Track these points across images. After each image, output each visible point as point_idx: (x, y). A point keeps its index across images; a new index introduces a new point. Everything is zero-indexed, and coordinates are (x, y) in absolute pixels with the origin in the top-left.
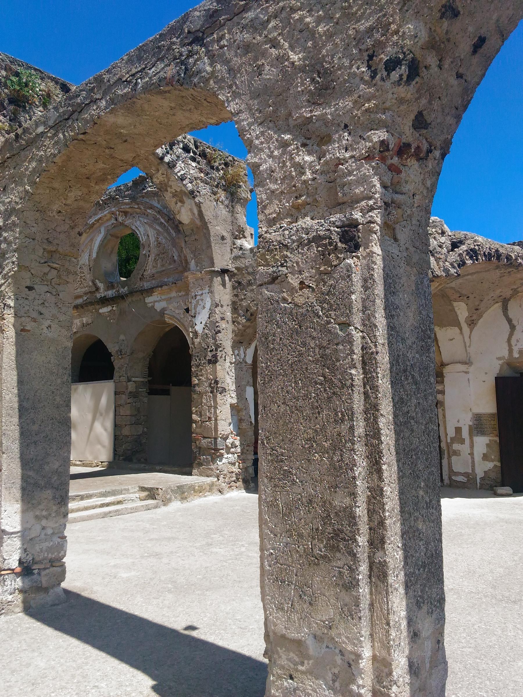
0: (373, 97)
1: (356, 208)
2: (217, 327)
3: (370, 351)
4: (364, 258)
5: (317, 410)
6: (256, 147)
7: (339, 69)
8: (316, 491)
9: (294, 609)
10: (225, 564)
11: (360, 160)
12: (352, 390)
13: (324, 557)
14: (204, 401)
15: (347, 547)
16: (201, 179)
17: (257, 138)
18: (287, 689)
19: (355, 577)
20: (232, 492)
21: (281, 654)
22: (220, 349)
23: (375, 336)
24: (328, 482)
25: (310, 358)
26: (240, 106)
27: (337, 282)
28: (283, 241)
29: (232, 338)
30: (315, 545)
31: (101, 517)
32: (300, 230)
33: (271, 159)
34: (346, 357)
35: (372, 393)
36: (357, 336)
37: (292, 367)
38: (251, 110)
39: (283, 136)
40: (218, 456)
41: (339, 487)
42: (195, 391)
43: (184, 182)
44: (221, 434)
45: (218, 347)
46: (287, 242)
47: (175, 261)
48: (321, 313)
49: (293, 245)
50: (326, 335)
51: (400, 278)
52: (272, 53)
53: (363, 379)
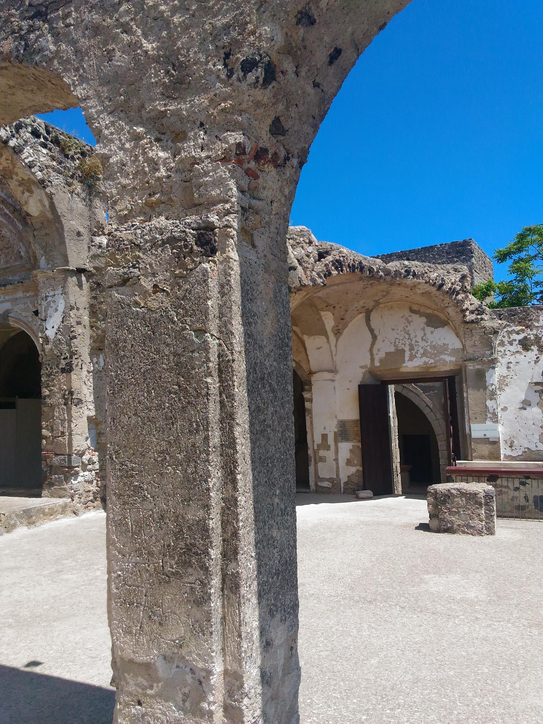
0: (229, 97)
1: (213, 210)
2: (72, 332)
3: (227, 359)
4: (221, 263)
5: (171, 420)
6: (106, 137)
7: (195, 64)
8: (168, 506)
9: (143, 632)
10: (76, 590)
11: (216, 161)
12: (208, 399)
13: (177, 573)
14: (56, 414)
15: (199, 561)
16: (53, 168)
17: (107, 128)
18: (135, 716)
19: (207, 592)
21: (129, 680)
22: (76, 356)
23: (232, 343)
24: (181, 496)
25: (164, 366)
26: (88, 92)
27: (193, 287)
28: (134, 241)
29: (90, 345)
30: (167, 562)
32: (153, 229)
33: (122, 152)
34: (202, 365)
35: (228, 402)
36: (213, 343)
37: (144, 376)
38: (100, 97)
39: (135, 128)
40: (72, 475)
41: (192, 500)
42: (45, 403)
43: (33, 170)
44: (76, 450)
45: (72, 354)
46: (139, 242)
47: (21, 257)
48: (176, 319)
49: (146, 245)
50: (181, 342)
51: (258, 285)
52: (124, 39)
53: (219, 387)
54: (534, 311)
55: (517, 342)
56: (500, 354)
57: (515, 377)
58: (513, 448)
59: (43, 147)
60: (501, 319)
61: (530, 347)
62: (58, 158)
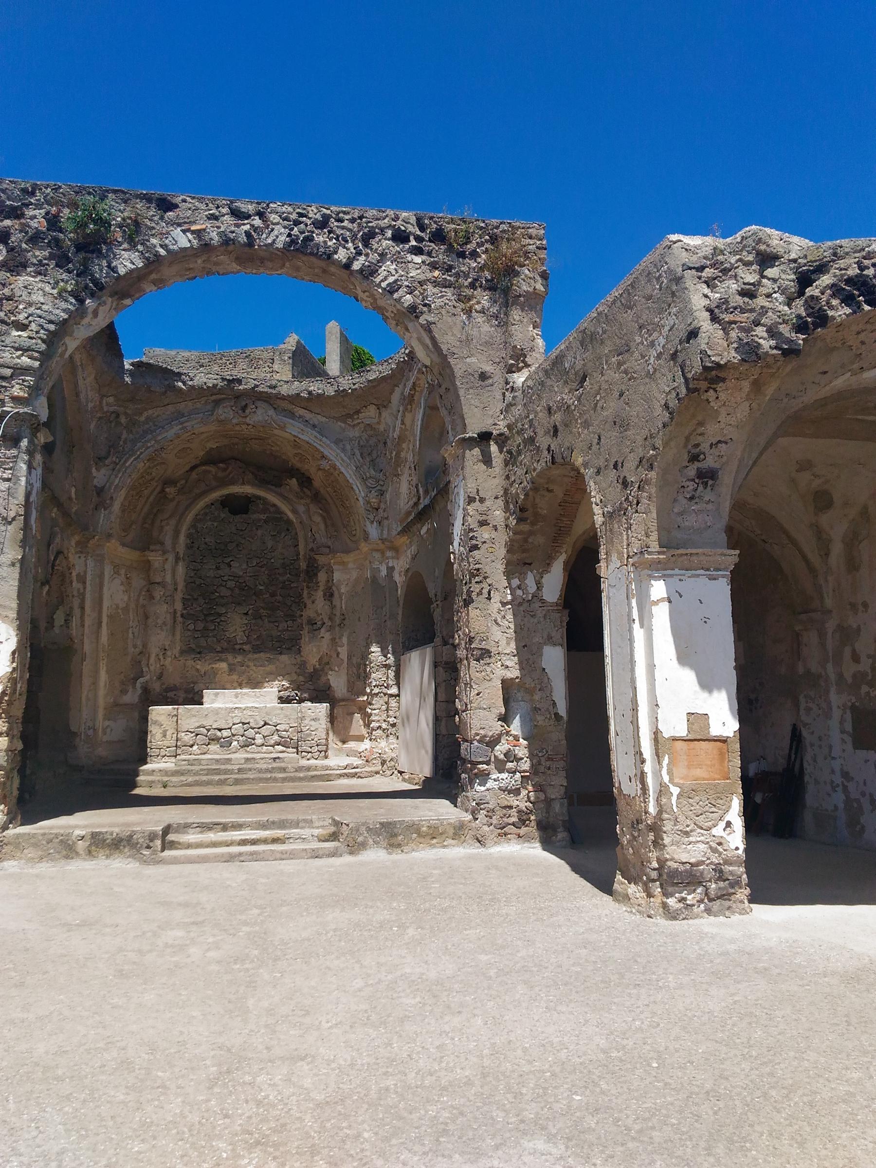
2: (471, 538)
20: (506, 845)
22: (477, 579)
31: (224, 860)
43: (396, 296)
59: (416, 255)
62: (445, 263)
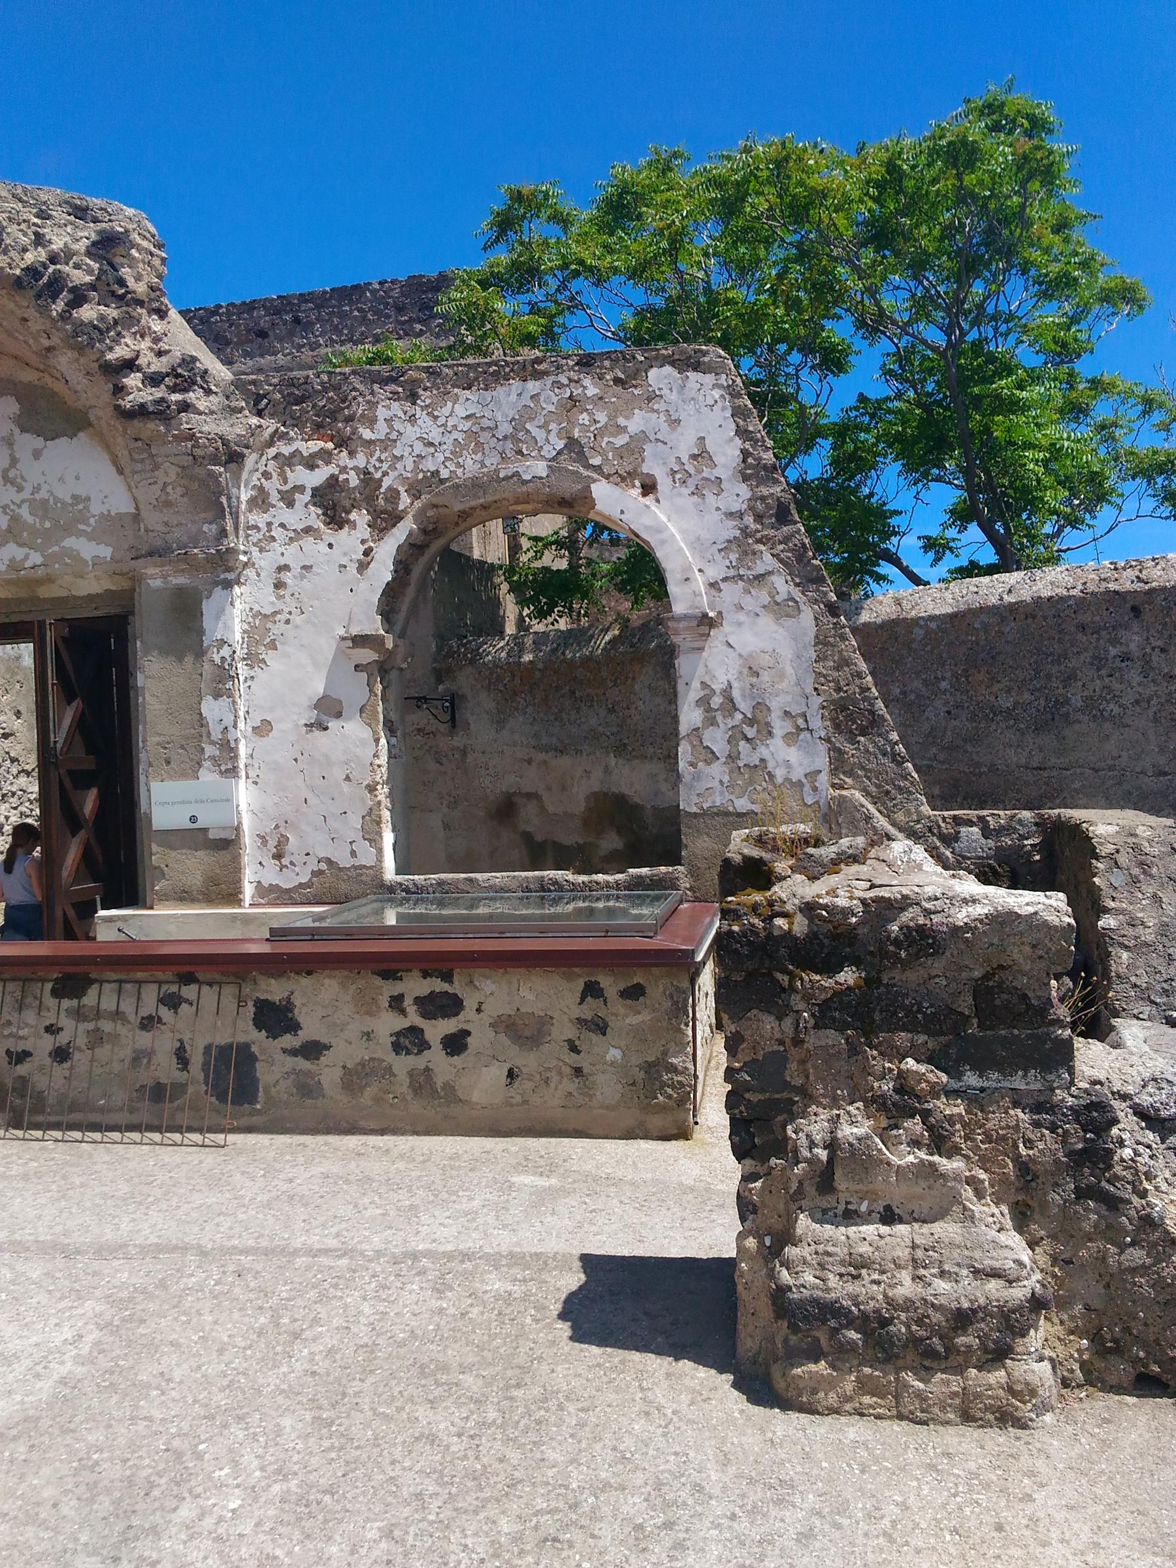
54: (361, 387)
55: (307, 496)
56: (255, 536)
57: (297, 619)
58: (285, 861)
60: (259, 414)
61: (348, 512)
